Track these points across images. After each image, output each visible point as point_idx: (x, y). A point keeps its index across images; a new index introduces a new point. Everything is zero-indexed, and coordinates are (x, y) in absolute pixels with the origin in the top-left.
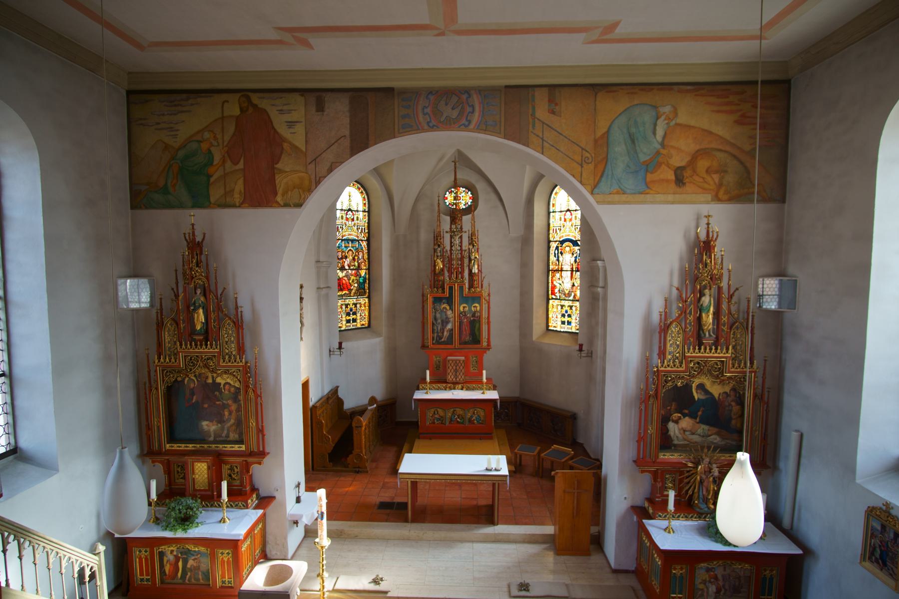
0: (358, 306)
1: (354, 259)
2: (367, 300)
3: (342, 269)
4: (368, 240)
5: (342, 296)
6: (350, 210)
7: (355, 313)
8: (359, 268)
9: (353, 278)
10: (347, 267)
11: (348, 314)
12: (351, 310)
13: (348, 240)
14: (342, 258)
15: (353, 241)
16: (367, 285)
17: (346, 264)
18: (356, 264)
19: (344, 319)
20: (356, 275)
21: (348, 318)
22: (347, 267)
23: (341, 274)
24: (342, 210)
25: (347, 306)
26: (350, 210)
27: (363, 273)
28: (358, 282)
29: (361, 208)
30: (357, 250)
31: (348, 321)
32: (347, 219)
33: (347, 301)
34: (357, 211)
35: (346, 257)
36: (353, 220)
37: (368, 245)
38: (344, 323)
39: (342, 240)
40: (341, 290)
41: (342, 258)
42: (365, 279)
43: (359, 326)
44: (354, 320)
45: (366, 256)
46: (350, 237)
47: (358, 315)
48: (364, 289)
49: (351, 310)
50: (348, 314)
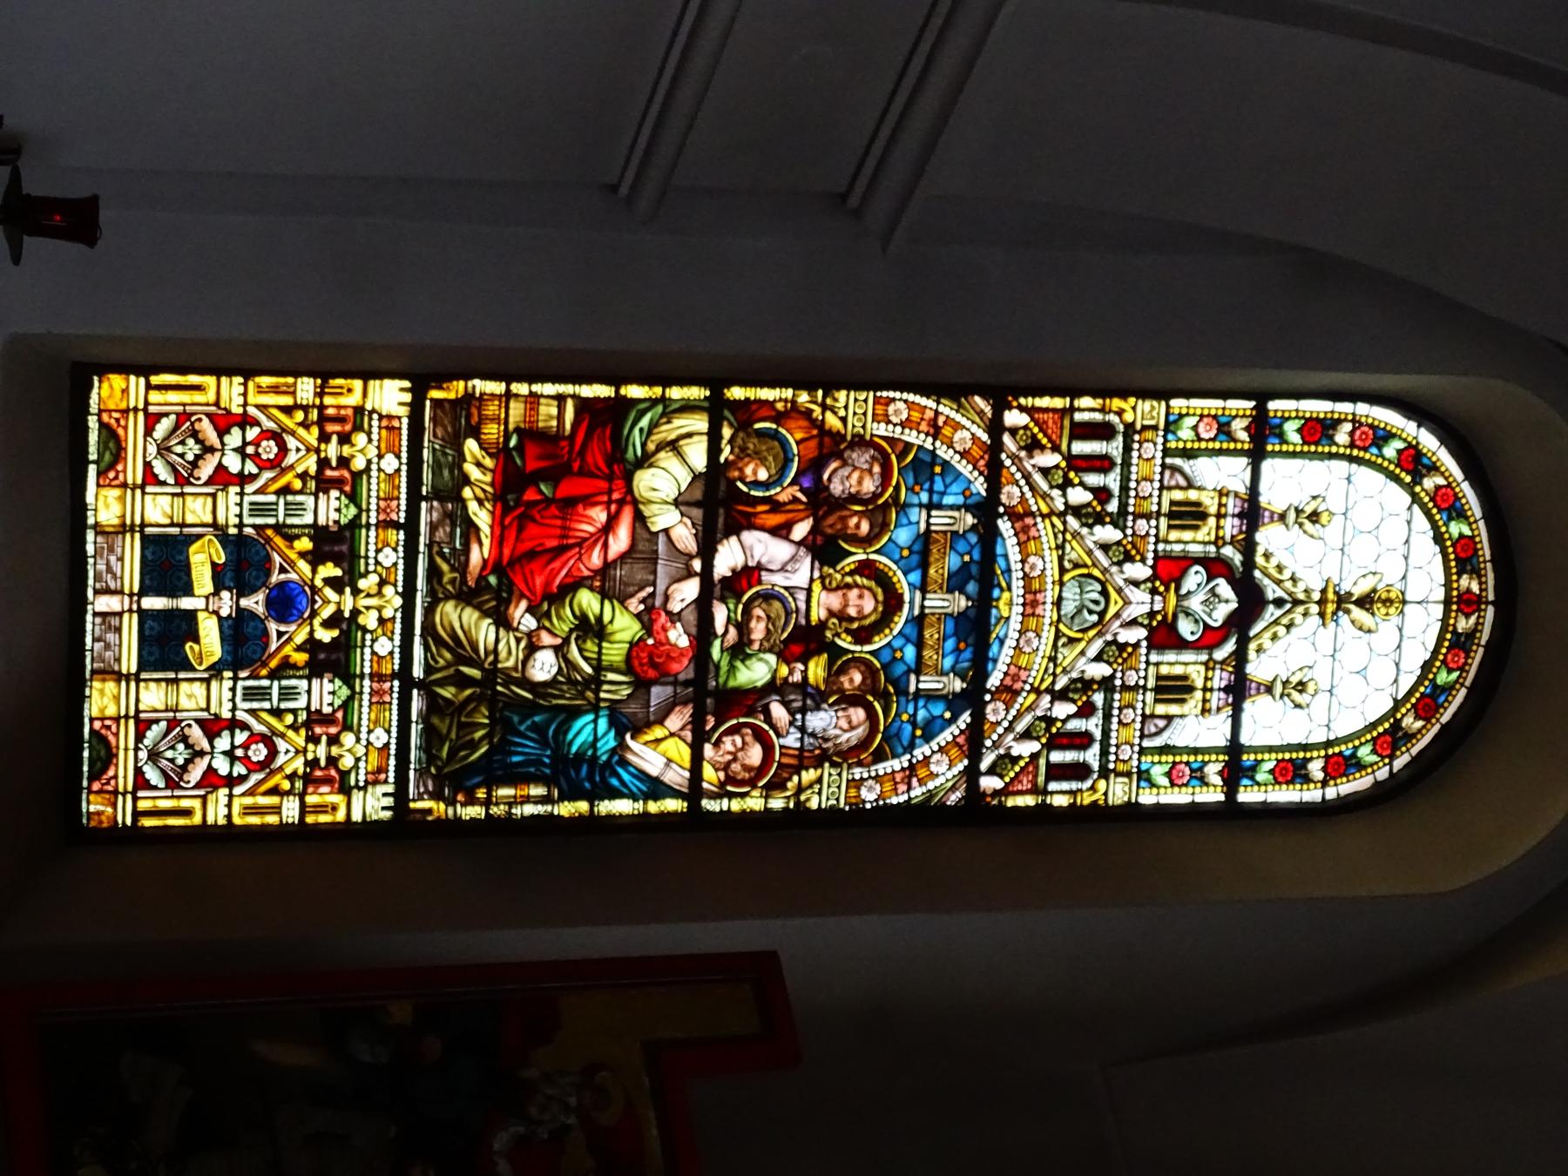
0: (325, 693)
1: (805, 640)
2: (373, 805)
3: (719, 505)
4: (977, 810)
5: (450, 492)
6: (1251, 601)
7: (243, 643)
8: (715, 705)
9: (624, 626)
10: (728, 558)
11: (244, 562)
12: (285, 603)
13: (982, 576)
14: (820, 502)
15: (975, 629)
16: (528, 802)
17: (761, 547)
18: (755, 672)
19: (197, 510)
20: (645, 664)
21: (202, 560)
22: (728, 558)
23: (662, 484)
24: (1252, 513)
25: (335, 545)
26: (1251, 601)
27: (661, 754)
28: (579, 690)
29: (1266, 723)
30: (884, 685)
31: (165, 561)
32: (1169, 570)
33: (383, 553)
34: (1239, 690)
35: (824, 550)
36: (1163, 635)
37: (927, 813)
38: (157, 509)
39: (986, 510)
40: (509, 487)
41: (820, 502)
42: (597, 776)
43: (101, 700)
44: (166, 644)
45: (825, 790)
46: (1009, 604)
47: (222, 697)
48: (497, 771)
49: (285, 603)
50: (244, 562)
